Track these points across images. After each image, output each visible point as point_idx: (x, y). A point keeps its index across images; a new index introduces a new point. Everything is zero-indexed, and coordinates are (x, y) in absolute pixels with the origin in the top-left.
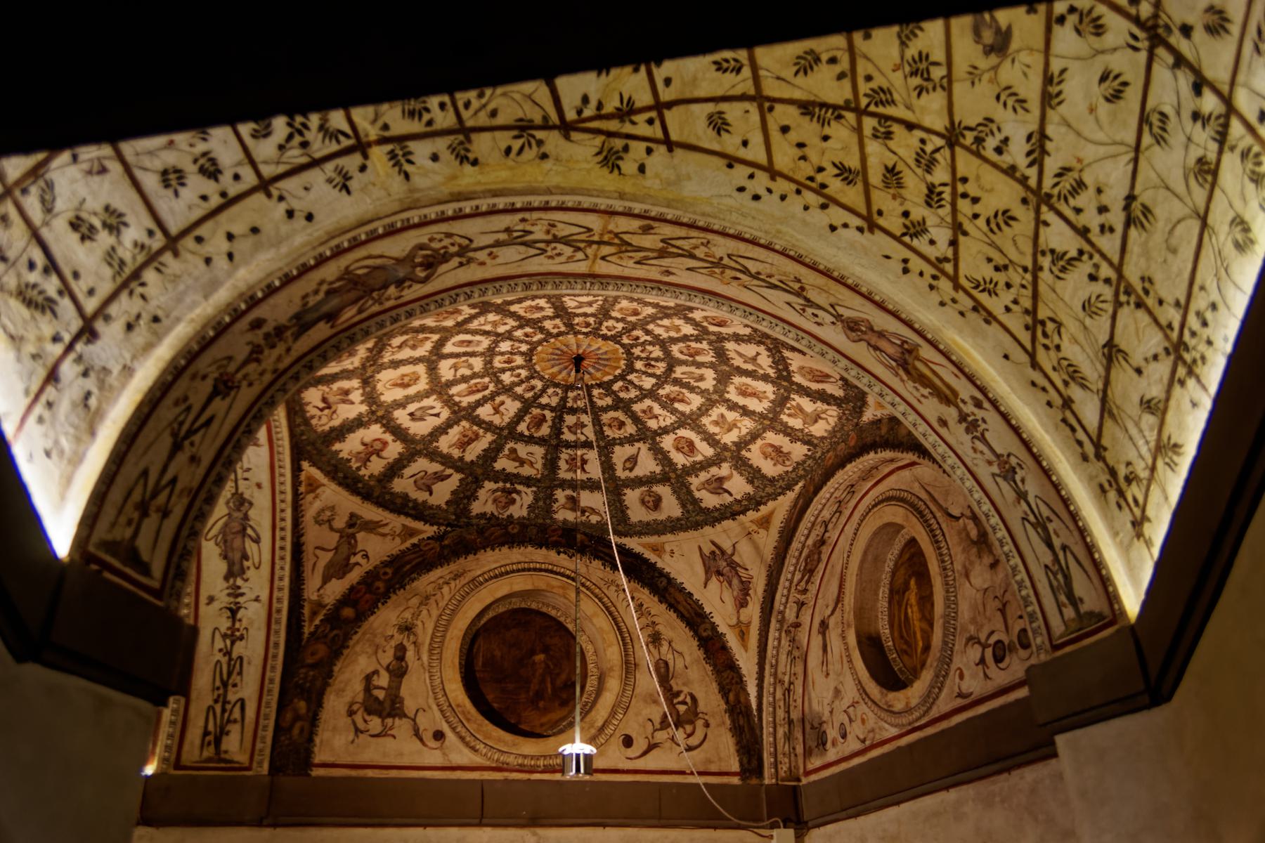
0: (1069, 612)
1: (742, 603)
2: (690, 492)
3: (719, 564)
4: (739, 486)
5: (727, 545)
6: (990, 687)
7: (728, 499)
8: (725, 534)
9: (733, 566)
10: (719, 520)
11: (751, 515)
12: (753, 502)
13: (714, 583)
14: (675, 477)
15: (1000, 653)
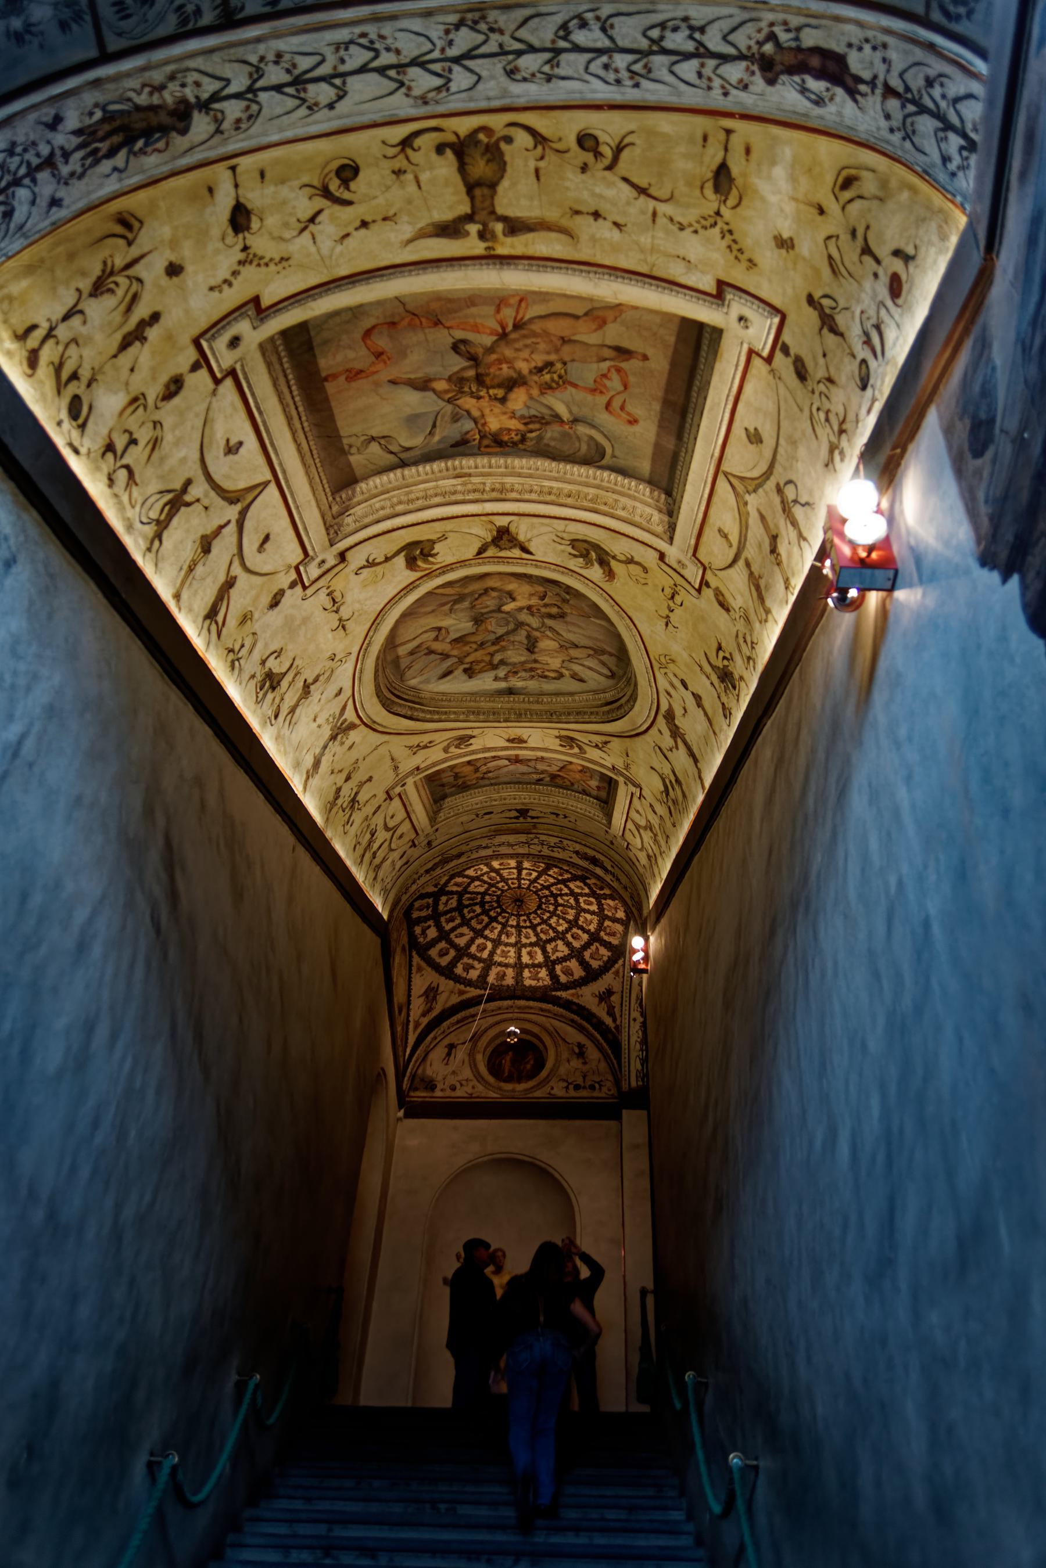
0: (640, 1083)
1: (424, 1015)
2: (458, 962)
3: (431, 994)
4: (474, 974)
5: (441, 989)
6: (568, 1095)
7: (464, 975)
8: (445, 985)
9: (435, 998)
10: (450, 979)
11: (462, 987)
12: (469, 983)
13: (422, 999)
14: (462, 952)
15: (577, 1087)
